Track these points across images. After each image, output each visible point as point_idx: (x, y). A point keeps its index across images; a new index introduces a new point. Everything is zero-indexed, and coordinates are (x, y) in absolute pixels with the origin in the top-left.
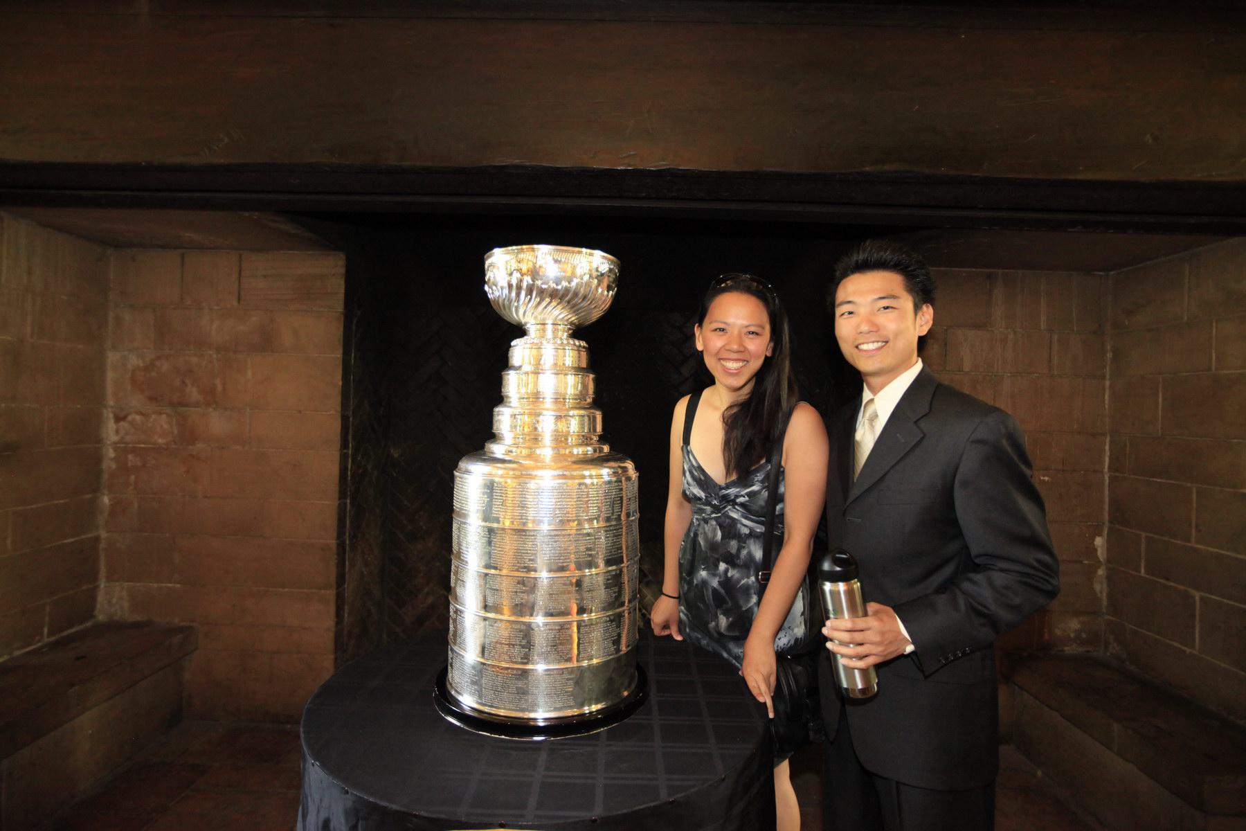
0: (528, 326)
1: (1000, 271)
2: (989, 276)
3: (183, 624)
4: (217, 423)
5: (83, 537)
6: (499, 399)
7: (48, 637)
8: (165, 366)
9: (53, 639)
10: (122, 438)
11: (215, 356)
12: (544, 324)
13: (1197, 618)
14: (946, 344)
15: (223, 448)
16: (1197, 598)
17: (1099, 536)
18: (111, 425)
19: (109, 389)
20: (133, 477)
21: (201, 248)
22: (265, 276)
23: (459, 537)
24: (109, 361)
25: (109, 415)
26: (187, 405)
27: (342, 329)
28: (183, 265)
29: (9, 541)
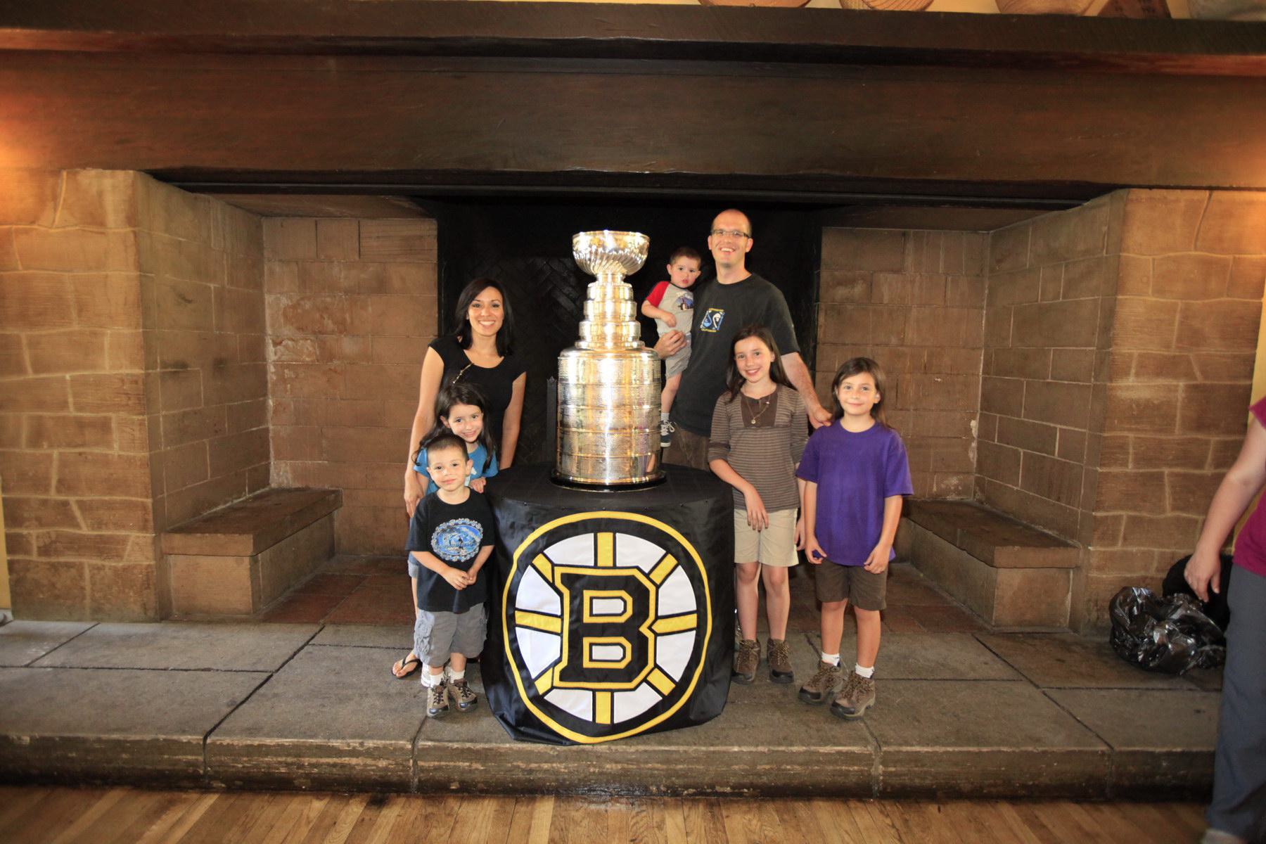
0: (598, 276)
1: (912, 231)
2: (904, 234)
4: (348, 346)
5: (261, 427)
6: (582, 317)
7: (250, 492)
8: (308, 305)
10: (280, 358)
11: (344, 297)
12: (607, 274)
13: (1021, 466)
14: (871, 285)
15: (353, 364)
16: (1022, 454)
20: (289, 386)
21: (330, 216)
23: (564, 392)
24: (266, 303)
25: (269, 341)
26: (323, 334)
28: (316, 230)
29: (226, 426)
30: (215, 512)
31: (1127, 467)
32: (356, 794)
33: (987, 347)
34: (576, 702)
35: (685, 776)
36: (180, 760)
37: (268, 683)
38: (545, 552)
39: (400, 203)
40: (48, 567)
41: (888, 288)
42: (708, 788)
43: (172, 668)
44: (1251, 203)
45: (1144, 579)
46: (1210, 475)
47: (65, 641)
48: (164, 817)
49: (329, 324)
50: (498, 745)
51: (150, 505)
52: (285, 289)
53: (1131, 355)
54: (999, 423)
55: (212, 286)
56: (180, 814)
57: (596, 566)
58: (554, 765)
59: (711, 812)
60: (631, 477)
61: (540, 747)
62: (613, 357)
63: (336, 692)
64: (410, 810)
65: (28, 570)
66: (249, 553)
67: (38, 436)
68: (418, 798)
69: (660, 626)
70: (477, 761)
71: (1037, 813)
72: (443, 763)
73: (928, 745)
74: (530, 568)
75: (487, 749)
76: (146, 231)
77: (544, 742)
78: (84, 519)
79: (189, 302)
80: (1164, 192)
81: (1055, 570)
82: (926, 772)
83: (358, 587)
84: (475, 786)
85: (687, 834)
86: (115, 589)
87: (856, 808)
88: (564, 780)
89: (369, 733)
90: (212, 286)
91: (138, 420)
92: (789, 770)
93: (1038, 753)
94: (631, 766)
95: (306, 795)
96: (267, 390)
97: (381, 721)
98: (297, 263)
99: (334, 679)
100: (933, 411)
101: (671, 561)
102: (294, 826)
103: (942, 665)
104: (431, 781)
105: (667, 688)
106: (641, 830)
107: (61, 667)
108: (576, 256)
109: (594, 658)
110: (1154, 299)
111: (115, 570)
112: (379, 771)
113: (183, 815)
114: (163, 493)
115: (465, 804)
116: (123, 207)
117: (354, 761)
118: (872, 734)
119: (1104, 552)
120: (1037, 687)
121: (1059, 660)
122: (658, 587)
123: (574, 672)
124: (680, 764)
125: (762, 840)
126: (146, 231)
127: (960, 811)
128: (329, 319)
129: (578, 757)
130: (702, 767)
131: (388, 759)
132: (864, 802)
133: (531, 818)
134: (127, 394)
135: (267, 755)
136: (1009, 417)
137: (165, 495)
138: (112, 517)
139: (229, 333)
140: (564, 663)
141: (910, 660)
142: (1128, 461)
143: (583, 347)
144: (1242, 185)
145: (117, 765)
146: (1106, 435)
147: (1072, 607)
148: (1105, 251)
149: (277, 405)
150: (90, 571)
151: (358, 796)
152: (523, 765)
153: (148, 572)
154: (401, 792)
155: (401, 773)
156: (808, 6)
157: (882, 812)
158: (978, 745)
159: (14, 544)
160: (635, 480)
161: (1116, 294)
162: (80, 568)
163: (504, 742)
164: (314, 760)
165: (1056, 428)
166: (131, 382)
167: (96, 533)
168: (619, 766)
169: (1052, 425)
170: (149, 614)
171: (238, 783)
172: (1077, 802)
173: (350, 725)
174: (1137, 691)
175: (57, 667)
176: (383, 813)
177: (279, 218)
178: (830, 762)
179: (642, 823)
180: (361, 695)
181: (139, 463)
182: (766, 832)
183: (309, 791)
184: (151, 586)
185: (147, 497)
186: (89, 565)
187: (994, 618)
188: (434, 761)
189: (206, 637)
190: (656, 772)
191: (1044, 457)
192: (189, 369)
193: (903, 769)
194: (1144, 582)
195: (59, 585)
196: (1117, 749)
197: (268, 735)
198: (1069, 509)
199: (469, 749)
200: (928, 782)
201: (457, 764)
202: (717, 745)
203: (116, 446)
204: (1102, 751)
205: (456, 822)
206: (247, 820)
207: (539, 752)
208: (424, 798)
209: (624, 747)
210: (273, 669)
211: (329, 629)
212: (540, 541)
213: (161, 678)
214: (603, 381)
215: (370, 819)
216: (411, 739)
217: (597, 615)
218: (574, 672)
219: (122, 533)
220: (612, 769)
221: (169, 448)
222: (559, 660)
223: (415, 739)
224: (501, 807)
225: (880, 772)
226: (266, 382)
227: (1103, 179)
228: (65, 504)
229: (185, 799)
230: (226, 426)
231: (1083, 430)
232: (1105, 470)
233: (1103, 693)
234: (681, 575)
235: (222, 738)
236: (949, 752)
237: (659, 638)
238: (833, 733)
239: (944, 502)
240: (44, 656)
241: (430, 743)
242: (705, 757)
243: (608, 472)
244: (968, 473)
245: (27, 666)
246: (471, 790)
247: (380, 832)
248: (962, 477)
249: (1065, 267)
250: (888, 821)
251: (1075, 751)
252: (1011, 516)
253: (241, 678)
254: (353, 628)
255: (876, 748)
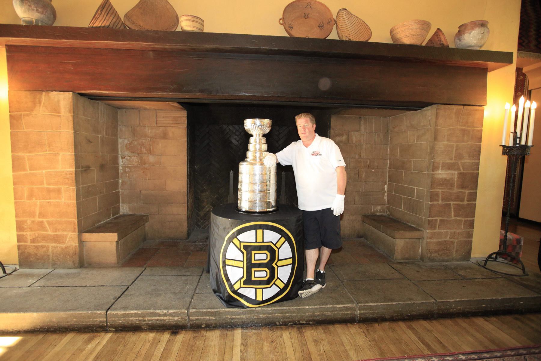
1: (363, 116)
3: (144, 214)
4: (151, 159)
5: (117, 191)
6: (248, 150)
7: (113, 216)
8: (136, 143)
9: (113, 217)
10: (124, 163)
12: (257, 134)
17: (386, 185)
18: (120, 160)
19: (119, 150)
20: (128, 174)
22: (164, 117)
24: (119, 142)
25: (120, 157)
26: (142, 154)
27: (186, 131)
28: (139, 114)
29: (104, 190)
30: (100, 225)
31: (439, 202)
32: (166, 330)
33: (390, 159)
34: (250, 292)
35: (289, 318)
36: (97, 320)
37: (127, 290)
38: (237, 237)
39: (175, 105)
40: (34, 247)
41: (355, 137)
42: (297, 322)
43: (88, 285)
44: (476, 110)
45: (445, 241)
46: (466, 204)
47: (42, 276)
48: (92, 342)
49: (144, 150)
50: (220, 310)
51: (77, 222)
52: (127, 137)
53: (439, 162)
54: (395, 186)
55: (99, 136)
56: (98, 341)
57: (256, 242)
58: (241, 316)
59: (299, 331)
60: (267, 209)
61: (236, 309)
62: (259, 165)
63: (155, 293)
64: (187, 335)
65: (26, 249)
66: (116, 240)
67: (30, 196)
68: (190, 331)
69: (279, 263)
70: (212, 316)
71: (412, 325)
72: (199, 317)
73: (374, 303)
74: (231, 243)
75: (216, 311)
76: (76, 115)
77: (236, 307)
78: (49, 228)
79: (91, 142)
80: (449, 106)
81: (415, 239)
82: (374, 312)
83: (157, 253)
84: (211, 325)
85: (291, 339)
86: (62, 256)
87: (350, 326)
88: (245, 321)
89: (170, 307)
90: (99, 136)
91: (72, 188)
92: (327, 314)
93: (412, 304)
94: (269, 315)
95: (146, 332)
96: (119, 176)
97: (174, 303)
98: (131, 127)
99: (153, 288)
100: (370, 182)
101: (283, 239)
102: (144, 343)
103: (378, 275)
104: (195, 324)
105: (282, 286)
106: (274, 338)
107: (43, 287)
108: (246, 128)
109: (255, 276)
110: (446, 143)
111: (62, 249)
112: (175, 321)
113: (99, 341)
114: (81, 217)
115: (208, 332)
116: (67, 106)
117: (165, 318)
118: (355, 300)
119: (432, 232)
120: (410, 281)
121: (417, 271)
122: (279, 249)
123: (249, 281)
124: (288, 313)
125: (318, 339)
126: (76, 115)
127: (386, 325)
128: (144, 148)
129: (250, 313)
130: (295, 314)
131: (178, 317)
132: (353, 324)
133: (233, 336)
134: (68, 179)
135: (131, 317)
136: (398, 184)
137: (82, 218)
138: (61, 227)
139: (105, 154)
140: (245, 278)
141: (366, 273)
142: (439, 200)
143: (248, 161)
144: (473, 104)
145: (72, 324)
146: (431, 191)
147: (421, 252)
148: (430, 126)
149: (123, 182)
150: (52, 249)
151: (167, 331)
152: (229, 317)
153: (75, 249)
154: (184, 329)
155: (183, 322)
156: (327, 38)
157: (359, 327)
158: (392, 302)
159: (20, 238)
160: (269, 210)
161: (434, 141)
162: (48, 247)
163: (221, 308)
164: (149, 318)
165: (415, 188)
166: (70, 174)
167: (54, 233)
168: (265, 316)
169: (413, 187)
170: (75, 265)
171: (120, 328)
172: (425, 320)
173: (163, 305)
174: (443, 281)
175: (41, 287)
176: (177, 337)
177: (124, 109)
178: (341, 310)
179: (274, 336)
180: (165, 293)
181: (72, 206)
182: (319, 337)
183: (148, 330)
184: (76, 254)
185: (75, 219)
186: (51, 246)
187: (395, 257)
188: (196, 317)
189: (100, 273)
190: (278, 317)
191: (410, 199)
192: (91, 168)
193: (366, 312)
194: (445, 242)
195: (38, 255)
196: (438, 301)
197: (131, 309)
198: (420, 217)
199: (209, 311)
200: (375, 316)
201: (205, 317)
202: (301, 306)
203: (63, 199)
204: (433, 302)
205: (205, 339)
206: (125, 342)
207: (236, 312)
208: (192, 331)
209: (267, 308)
210: (129, 285)
211: (148, 269)
212: (235, 233)
213: (85, 290)
214: (256, 174)
215: (173, 339)
216: (187, 309)
217: (257, 260)
218: (249, 281)
219: (65, 233)
220: (262, 316)
221: (83, 200)
222: (243, 277)
223: (188, 308)
224: (222, 332)
225: (358, 313)
226: (118, 173)
227: (430, 101)
228: (42, 222)
229: (99, 335)
230: (104, 190)
231: (424, 189)
232: (432, 203)
233: (433, 282)
234: (287, 244)
235: (114, 311)
236: (382, 305)
237: (279, 268)
238: (341, 300)
239: (376, 215)
240: (35, 282)
241: (194, 310)
242: (296, 311)
243: (257, 207)
244: (384, 205)
245: (29, 287)
246: (210, 327)
247: (177, 344)
248: (382, 206)
249: (417, 131)
250: (361, 330)
251: (424, 302)
252: (399, 220)
253: (117, 288)
254: (158, 268)
255: (357, 306)
